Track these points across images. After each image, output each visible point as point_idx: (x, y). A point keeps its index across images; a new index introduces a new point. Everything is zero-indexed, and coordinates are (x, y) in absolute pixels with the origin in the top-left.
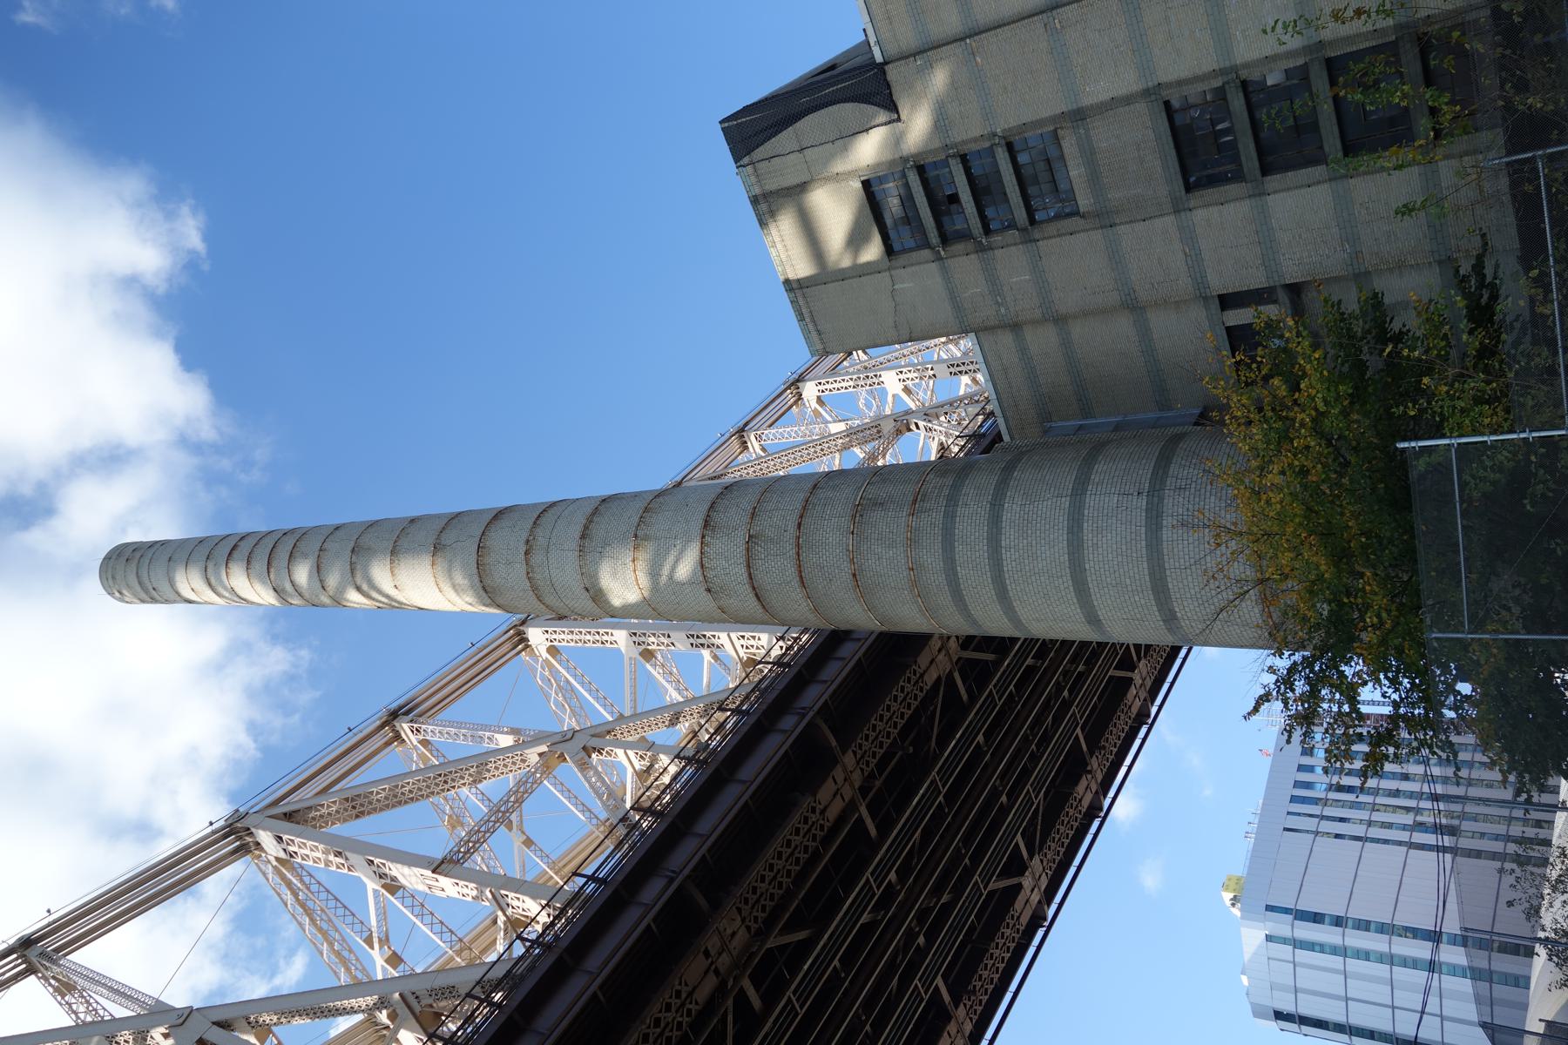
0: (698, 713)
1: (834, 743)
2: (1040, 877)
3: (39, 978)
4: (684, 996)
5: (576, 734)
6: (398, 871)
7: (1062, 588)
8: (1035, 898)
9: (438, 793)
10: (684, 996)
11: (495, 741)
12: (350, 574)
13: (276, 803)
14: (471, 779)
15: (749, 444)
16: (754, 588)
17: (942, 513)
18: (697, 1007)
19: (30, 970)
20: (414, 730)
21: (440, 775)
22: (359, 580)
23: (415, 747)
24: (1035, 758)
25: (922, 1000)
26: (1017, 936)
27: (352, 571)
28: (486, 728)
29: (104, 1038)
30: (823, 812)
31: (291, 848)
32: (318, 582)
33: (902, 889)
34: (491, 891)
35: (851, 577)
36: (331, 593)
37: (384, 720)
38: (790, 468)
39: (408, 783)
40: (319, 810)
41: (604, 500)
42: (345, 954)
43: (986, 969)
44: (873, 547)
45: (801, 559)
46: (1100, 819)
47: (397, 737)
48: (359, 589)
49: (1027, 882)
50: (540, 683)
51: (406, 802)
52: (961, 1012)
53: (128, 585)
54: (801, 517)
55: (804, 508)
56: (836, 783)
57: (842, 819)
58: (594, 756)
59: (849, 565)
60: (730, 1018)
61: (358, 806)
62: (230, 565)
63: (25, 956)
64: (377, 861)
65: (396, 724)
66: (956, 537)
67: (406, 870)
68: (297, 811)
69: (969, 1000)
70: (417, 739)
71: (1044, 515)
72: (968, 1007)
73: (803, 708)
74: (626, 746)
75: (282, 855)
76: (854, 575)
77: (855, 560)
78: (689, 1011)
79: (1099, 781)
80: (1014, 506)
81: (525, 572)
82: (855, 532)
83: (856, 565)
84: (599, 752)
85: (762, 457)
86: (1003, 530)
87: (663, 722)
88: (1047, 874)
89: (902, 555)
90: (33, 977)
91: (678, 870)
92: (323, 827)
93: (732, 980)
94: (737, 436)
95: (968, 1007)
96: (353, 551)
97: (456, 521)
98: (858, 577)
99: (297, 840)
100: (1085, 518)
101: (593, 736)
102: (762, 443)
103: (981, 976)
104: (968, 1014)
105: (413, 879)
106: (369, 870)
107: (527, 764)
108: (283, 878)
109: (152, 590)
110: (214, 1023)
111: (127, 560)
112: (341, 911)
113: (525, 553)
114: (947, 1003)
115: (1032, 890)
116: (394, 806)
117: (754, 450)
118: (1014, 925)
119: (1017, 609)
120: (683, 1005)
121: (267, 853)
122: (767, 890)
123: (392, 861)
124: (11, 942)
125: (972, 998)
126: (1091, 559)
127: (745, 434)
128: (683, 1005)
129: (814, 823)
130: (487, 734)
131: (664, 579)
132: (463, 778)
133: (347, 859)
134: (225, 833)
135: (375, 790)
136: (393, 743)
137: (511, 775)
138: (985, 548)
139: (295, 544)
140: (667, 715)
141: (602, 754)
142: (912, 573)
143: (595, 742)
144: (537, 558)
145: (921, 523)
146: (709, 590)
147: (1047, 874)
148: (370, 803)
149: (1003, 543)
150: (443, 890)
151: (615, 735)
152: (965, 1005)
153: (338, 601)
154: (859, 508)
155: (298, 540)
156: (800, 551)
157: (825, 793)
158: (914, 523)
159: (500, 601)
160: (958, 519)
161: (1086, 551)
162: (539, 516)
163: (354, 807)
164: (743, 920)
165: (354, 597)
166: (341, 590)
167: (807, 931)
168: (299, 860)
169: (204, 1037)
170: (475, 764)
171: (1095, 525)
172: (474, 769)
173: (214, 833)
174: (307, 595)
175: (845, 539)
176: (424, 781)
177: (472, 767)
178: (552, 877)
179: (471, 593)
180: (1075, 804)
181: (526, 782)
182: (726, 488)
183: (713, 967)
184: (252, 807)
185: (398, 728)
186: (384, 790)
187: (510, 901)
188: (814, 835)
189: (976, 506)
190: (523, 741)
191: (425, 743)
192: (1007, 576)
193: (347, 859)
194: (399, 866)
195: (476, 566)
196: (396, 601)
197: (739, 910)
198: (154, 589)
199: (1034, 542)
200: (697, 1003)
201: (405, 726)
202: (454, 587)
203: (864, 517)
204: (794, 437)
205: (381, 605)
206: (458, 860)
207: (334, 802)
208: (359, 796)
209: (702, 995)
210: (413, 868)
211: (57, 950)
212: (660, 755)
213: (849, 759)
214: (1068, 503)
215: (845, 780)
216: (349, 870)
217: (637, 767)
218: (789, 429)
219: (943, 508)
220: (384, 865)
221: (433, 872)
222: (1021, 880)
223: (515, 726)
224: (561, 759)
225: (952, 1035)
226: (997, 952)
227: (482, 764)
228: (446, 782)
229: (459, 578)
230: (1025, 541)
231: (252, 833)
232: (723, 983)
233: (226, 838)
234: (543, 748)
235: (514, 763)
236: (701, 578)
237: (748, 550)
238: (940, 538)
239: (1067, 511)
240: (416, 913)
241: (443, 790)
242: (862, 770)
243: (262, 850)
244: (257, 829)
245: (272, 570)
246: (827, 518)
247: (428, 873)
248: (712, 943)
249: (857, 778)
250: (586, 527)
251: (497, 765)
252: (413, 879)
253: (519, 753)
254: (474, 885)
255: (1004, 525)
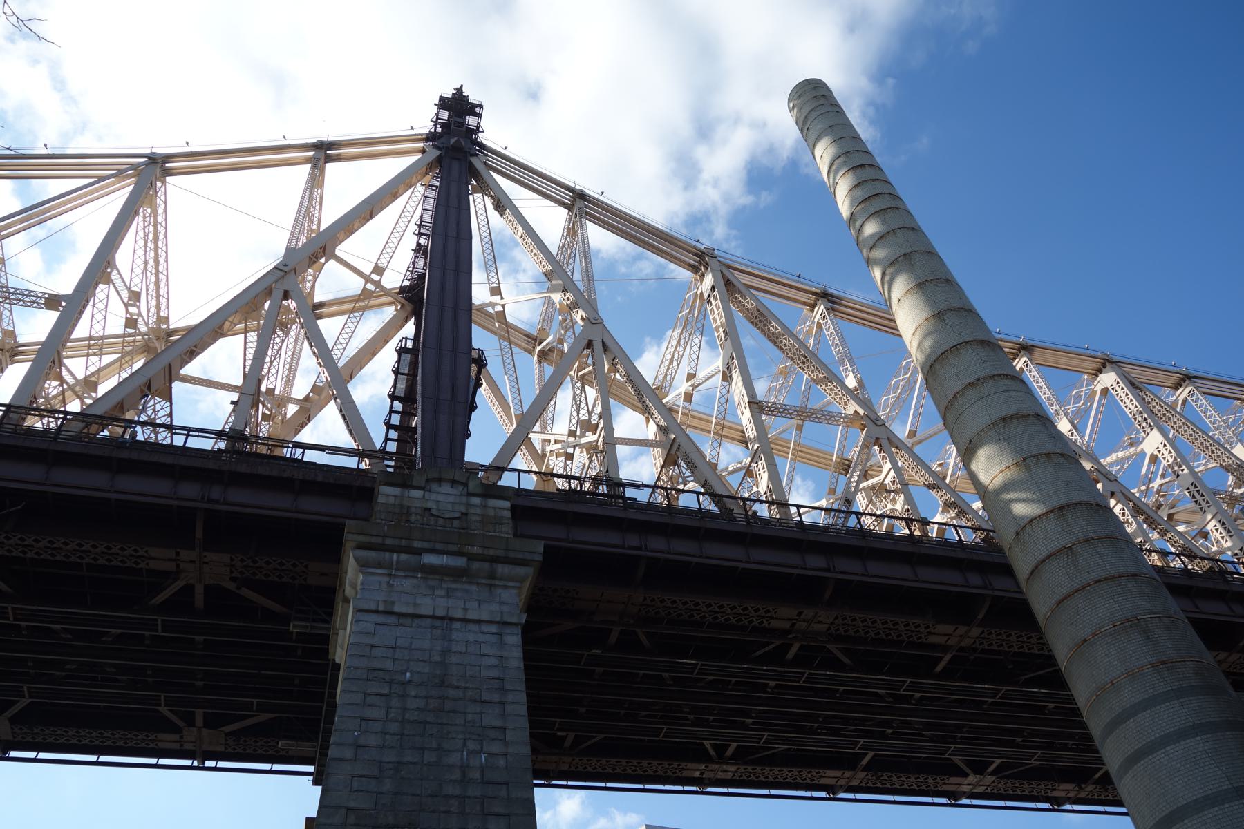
0: (946, 500)
1: (980, 616)
2: (982, 785)
3: (568, 213)
4: (769, 615)
5: (883, 426)
6: (737, 376)
7: (1161, 806)
8: (965, 788)
9: (795, 362)
10: (769, 615)
11: (847, 374)
12: (889, 263)
13: (729, 267)
14: (815, 377)
15: (1181, 390)
16: (1036, 567)
17: (1166, 690)
18: (767, 625)
19: (569, 208)
20: (823, 315)
21: (806, 357)
22: (889, 271)
23: (813, 322)
24: (1065, 748)
25: (853, 749)
26: (932, 787)
27: (892, 264)
28: (852, 363)
29: (563, 286)
30: (930, 633)
31: (712, 299)
32: (872, 243)
33: (914, 705)
34: (758, 447)
35: (1083, 639)
36: (871, 255)
37: (818, 291)
38: (1180, 436)
39: (789, 341)
40: (742, 299)
41: (1038, 415)
42: (675, 363)
43: (898, 778)
44: (1112, 646)
45: (1076, 594)
46: (1051, 807)
47: (813, 306)
48: (883, 274)
49: (972, 778)
50: (903, 365)
51: (778, 346)
52: (862, 775)
53: (800, 109)
54: (1106, 579)
55: (1114, 577)
56: (955, 631)
57: (934, 646)
58: (876, 448)
59: (1090, 633)
60: (773, 646)
61: (759, 319)
62: (850, 172)
63: (575, 200)
64: (735, 361)
65: (820, 300)
66: (1154, 709)
67: (740, 384)
68: (735, 286)
69: (872, 776)
70: (819, 320)
71: (1206, 772)
72: (867, 777)
73: (991, 584)
74: (894, 465)
75: (706, 296)
76: (1085, 641)
77: (1096, 637)
78: (762, 622)
79: (1079, 796)
80: (1201, 745)
81: (958, 390)
82: (1116, 628)
83: (1092, 639)
84: (881, 450)
85: (1175, 410)
86: (1177, 745)
87: (926, 480)
88: (987, 789)
89: (1118, 672)
90: (567, 211)
91: (837, 570)
92: (734, 306)
93: (794, 635)
94: (1181, 376)
95: (867, 777)
96: (905, 255)
97: (964, 313)
98: (1085, 644)
99: (719, 301)
100: (1222, 807)
101: (888, 439)
102: (1189, 399)
103: (891, 776)
104: (863, 779)
105: (737, 391)
106: (728, 359)
107: (845, 407)
108: (694, 301)
109: (806, 128)
110: (603, 341)
111: (815, 97)
112: (695, 349)
113: (970, 383)
114: (861, 763)
115: (969, 785)
116: (771, 340)
117: (1180, 394)
118: (938, 783)
119: (1128, 775)
120: (763, 617)
121: (701, 285)
122: (859, 627)
123: (740, 371)
124: (577, 187)
125: (874, 778)
126: (1193, 823)
127: (1187, 382)
128: (763, 617)
129: (919, 631)
130: (848, 366)
131: (1007, 496)
132: (813, 372)
133: (726, 340)
134: (697, 254)
135: (774, 323)
136: (808, 306)
137: (829, 397)
138: (1158, 735)
139: (887, 209)
140: (931, 479)
141: (880, 453)
142: (1110, 685)
143: (885, 443)
144: (972, 394)
145: (1149, 677)
146: (1017, 534)
147: (987, 789)
148: (765, 326)
149: (1168, 748)
150: (742, 414)
151: (897, 453)
152: (867, 775)
153: (869, 262)
154: (1136, 621)
155: (890, 208)
156: (1080, 592)
157: (942, 628)
158: (1147, 671)
159: (930, 380)
160: (1168, 704)
161: (1196, 817)
162: (1000, 375)
163: (756, 317)
164: (832, 623)
165: (877, 273)
166: (877, 262)
167: (849, 662)
168: (709, 309)
169: (594, 342)
170: (825, 375)
171: (1220, 817)
172: (822, 376)
173: (694, 247)
174: (860, 239)
175: (1107, 622)
176: (797, 349)
177: (823, 374)
178: (790, 448)
179: (923, 357)
180: (1050, 787)
181: (834, 417)
182: (1097, 505)
183: (794, 621)
184: (721, 257)
185: (819, 303)
186: (777, 329)
187: (760, 463)
188: (911, 636)
189: (1185, 714)
190: (858, 393)
191: (819, 326)
192: (1146, 760)
193: (726, 340)
194: (740, 378)
195: (943, 351)
196: (890, 303)
197: (836, 618)
198: (808, 128)
199: (1182, 772)
200: (769, 624)
201: (822, 307)
202: (920, 343)
203: (1131, 629)
204: (1210, 422)
205: (882, 291)
206: (764, 410)
207: (752, 305)
208: (764, 316)
209: (775, 624)
210: (744, 388)
211: (587, 213)
212: (902, 495)
213: (976, 631)
214: (1226, 787)
215: (961, 636)
216: (721, 345)
217: (886, 482)
218: (1214, 413)
219: (1170, 688)
220: (735, 368)
221: (748, 402)
222: (971, 774)
223: (865, 382)
224: (862, 427)
225: (844, 776)
226: (912, 779)
227: (828, 379)
228: (804, 363)
229: (928, 344)
230: (1179, 765)
231: (707, 268)
232: (789, 632)
233: (695, 255)
234: (861, 412)
235: (841, 398)
236: (1022, 524)
237: (1060, 550)
238: (1147, 696)
239: (1220, 789)
240: (720, 400)
241: (798, 364)
242: (975, 642)
243: (702, 281)
244: (711, 271)
245: (863, 205)
246: (1116, 600)
247: (747, 400)
248: (808, 613)
249: (966, 643)
250: (1011, 417)
251: (833, 388)
252: (737, 391)
253: (849, 398)
254: (755, 433)
255: (1183, 743)
